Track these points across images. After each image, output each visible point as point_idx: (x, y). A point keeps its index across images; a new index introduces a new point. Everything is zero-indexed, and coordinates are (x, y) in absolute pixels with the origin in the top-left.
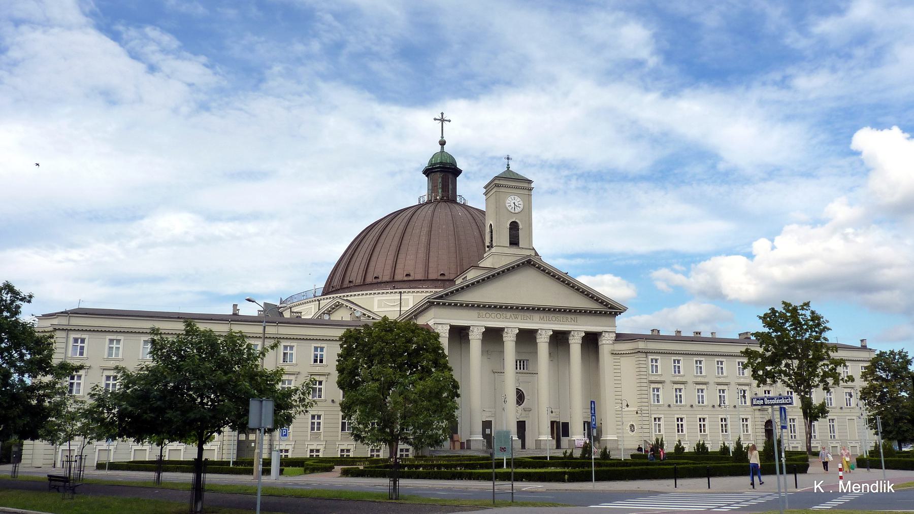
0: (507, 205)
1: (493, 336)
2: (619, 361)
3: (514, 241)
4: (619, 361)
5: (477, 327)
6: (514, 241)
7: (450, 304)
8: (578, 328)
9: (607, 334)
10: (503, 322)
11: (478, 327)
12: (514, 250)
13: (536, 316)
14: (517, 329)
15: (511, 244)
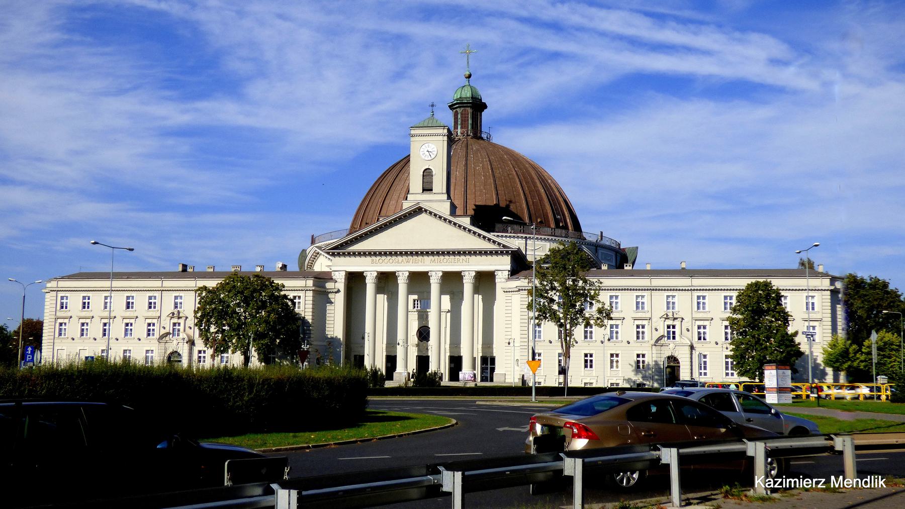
0: (421, 153)
1: (386, 281)
2: (510, 298)
3: (427, 189)
4: (510, 298)
5: (370, 272)
6: (427, 189)
7: (344, 254)
8: (469, 267)
9: (500, 272)
10: (396, 266)
11: (371, 272)
12: (427, 196)
13: (427, 259)
14: (407, 272)
15: (424, 190)
